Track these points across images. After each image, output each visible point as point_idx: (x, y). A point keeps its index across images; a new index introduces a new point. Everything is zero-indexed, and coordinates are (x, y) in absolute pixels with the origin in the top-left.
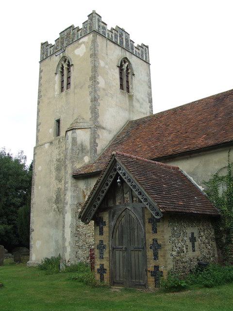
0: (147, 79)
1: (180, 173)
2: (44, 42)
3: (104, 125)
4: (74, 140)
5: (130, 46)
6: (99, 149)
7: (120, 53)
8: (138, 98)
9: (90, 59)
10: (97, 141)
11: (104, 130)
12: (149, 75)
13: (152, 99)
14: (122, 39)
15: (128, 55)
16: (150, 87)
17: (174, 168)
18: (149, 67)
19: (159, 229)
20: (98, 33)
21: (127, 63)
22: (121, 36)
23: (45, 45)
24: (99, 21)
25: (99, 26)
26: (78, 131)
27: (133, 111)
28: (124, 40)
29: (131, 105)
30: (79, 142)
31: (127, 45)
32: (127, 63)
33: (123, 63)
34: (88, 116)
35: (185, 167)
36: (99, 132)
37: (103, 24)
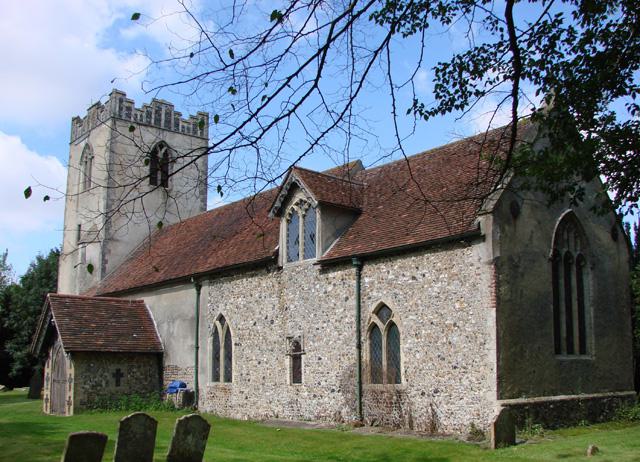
1: (144, 306)
2: (76, 116)
4: (84, 255)
5: (173, 121)
14: (160, 115)
17: (134, 302)
21: (165, 148)
22: (158, 112)
24: (121, 101)
25: (121, 109)
28: (163, 117)
31: (168, 122)
32: (165, 148)
35: (149, 301)
36: (110, 246)
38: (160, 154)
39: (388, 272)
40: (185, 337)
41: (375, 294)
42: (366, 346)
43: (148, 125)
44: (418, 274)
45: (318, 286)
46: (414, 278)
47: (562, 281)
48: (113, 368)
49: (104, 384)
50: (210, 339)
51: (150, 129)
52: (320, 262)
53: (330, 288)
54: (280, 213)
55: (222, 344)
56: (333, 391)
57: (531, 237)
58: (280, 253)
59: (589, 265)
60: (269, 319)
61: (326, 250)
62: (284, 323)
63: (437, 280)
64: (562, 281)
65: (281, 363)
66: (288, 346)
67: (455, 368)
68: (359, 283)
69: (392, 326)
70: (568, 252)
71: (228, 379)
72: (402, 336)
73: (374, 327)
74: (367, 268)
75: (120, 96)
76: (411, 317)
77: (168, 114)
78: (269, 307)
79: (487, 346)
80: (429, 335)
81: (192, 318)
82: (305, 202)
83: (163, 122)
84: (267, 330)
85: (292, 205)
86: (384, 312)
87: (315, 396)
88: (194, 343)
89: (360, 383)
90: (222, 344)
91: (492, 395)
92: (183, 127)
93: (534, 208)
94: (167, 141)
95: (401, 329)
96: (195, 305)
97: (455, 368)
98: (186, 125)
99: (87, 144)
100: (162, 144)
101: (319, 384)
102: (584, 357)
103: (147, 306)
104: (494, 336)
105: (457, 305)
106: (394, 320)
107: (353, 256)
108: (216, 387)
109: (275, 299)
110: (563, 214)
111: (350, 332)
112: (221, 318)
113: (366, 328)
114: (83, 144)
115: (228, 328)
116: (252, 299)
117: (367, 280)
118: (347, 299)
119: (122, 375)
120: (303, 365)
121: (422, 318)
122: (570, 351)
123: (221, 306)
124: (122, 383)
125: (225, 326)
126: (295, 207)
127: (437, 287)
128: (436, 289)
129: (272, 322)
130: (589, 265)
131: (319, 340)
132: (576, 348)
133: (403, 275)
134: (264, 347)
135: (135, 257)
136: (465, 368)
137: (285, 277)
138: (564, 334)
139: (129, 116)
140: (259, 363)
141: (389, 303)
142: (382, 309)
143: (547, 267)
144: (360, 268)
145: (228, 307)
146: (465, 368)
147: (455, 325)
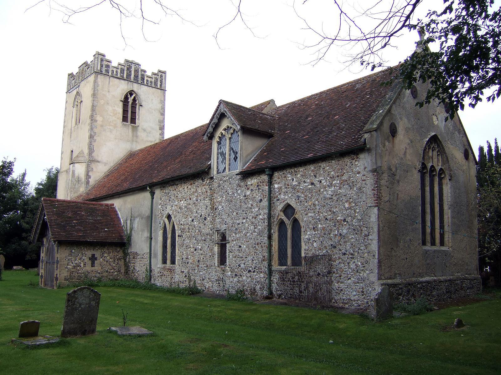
0: (159, 106)
1: (114, 208)
2: (70, 73)
3: (99, 159)
4: (73, 172)
5: (140, 76)
6: (92, 181)
7: (126, 87)
8: (145, 127)
9: (91, 99)
10: (90, 174)
11: (98, 164)
12: (163, 102)
13: (164, 126)
15: (135, 87)
16: (163, 114)
17: (107, 205)
18: (164, 93)
19: (59, 251)
20: (101, 73)
21: (134, 95)
22: (129, 69)
23: (71, 75)
24: (102, 60)
25: (102, 66)
26: (76, 165)
27: (136, 142)
29: (135, 136)
30: (76, 175)
31: (136, 77)
32: (134, 95)
33: (129, 96)
34: (86, 151)
35: (117, 203)
36: (93, 165)
37: (107, 63)
38: (130, 100)
39: (293, 180)
40: (143, 231)
41: (282, 196)
42: (275, 236)
43: (122, 78)
44: (316, 181)
45: (239, 191)
46: (312, 184)
47: (428, 189)
48: (89, 253)
49: (82, 265)
50: (160, 233)
51: (122, 81)
52: (241, 173)
53: (248, 193)
54: (211, 137)
55: (169, 236)
56: (250, 271)
57: (405, 152)
58: (212, 167)
59: (448, 177)
60: (203, 217)
61: (246, 164)
62: (214, 220)
63: (331, 185)
64: (428, 189)
65: (211, 250)
66: (216, 237)
67: (345, 254)
68: (270, 188)
69: (296, 222)
70: (432, 166)
71: (173, 262)
72: (303, 230)
73: (282, 224)
74: (276, 174)
75: (100, 57)
76: (310, 214)
77: (136, 71)
78: (203, 208)
79: (370, 237)
80: (324, 228)
81: (148, 217)
82: (231, 128)
83: (132, 76)
84: (201, 225)
85: (221, 130)
86: (289, 211)
87: (236, 275)
88: (149, 235)
89: (270, 265)
90: (169, 236)
91: (374, 277)
92: (147, 81)
93: (407, 130)
94: (135, 90)
95: (302, 224)
96: (150, 207)
97: (345, 254)
98: (149, 79)
99: (77, 92)
100: (131, 93)
101: (239, 266)
102: (443, 248)
103: (117, 208)
104: (376, 230)
105: (347, 205)
106: (297, 216)
107: (267, 168)
108: (164, 268)
109: (207, 202)
110: (430, 136)
111: (262, 226)
112: (169, 217)
113: (276, 223)
114: (75, 92)
115: (174, 225)
116: (191, 202)
117: (276, 186)
118: (261, 200)
119: (96, 259)
120: (227, 251)
121: (319, 215)
122: (433, 243)
123: (169, 207)
124: (96, 265)
125: (172, 224)
126: (223, 132)
127: (330, 191)
128: (330, 193)
129: (205, 219)
130: (448, 177)
131: (240, 232)
132: (438, 241)
133: (305, 182)
134: (199, 238)
135: (109, 175)
136: (352, 254)
137: (215, 185)
138: (428, 230)
139: (107, 71)
140: (196, 250)
141: (293, 204)
142: (288, 209)
143: (417, 176)
144: (271, 176)
145: (173, 208)
146: (352, 254)
147: (345, 220)
